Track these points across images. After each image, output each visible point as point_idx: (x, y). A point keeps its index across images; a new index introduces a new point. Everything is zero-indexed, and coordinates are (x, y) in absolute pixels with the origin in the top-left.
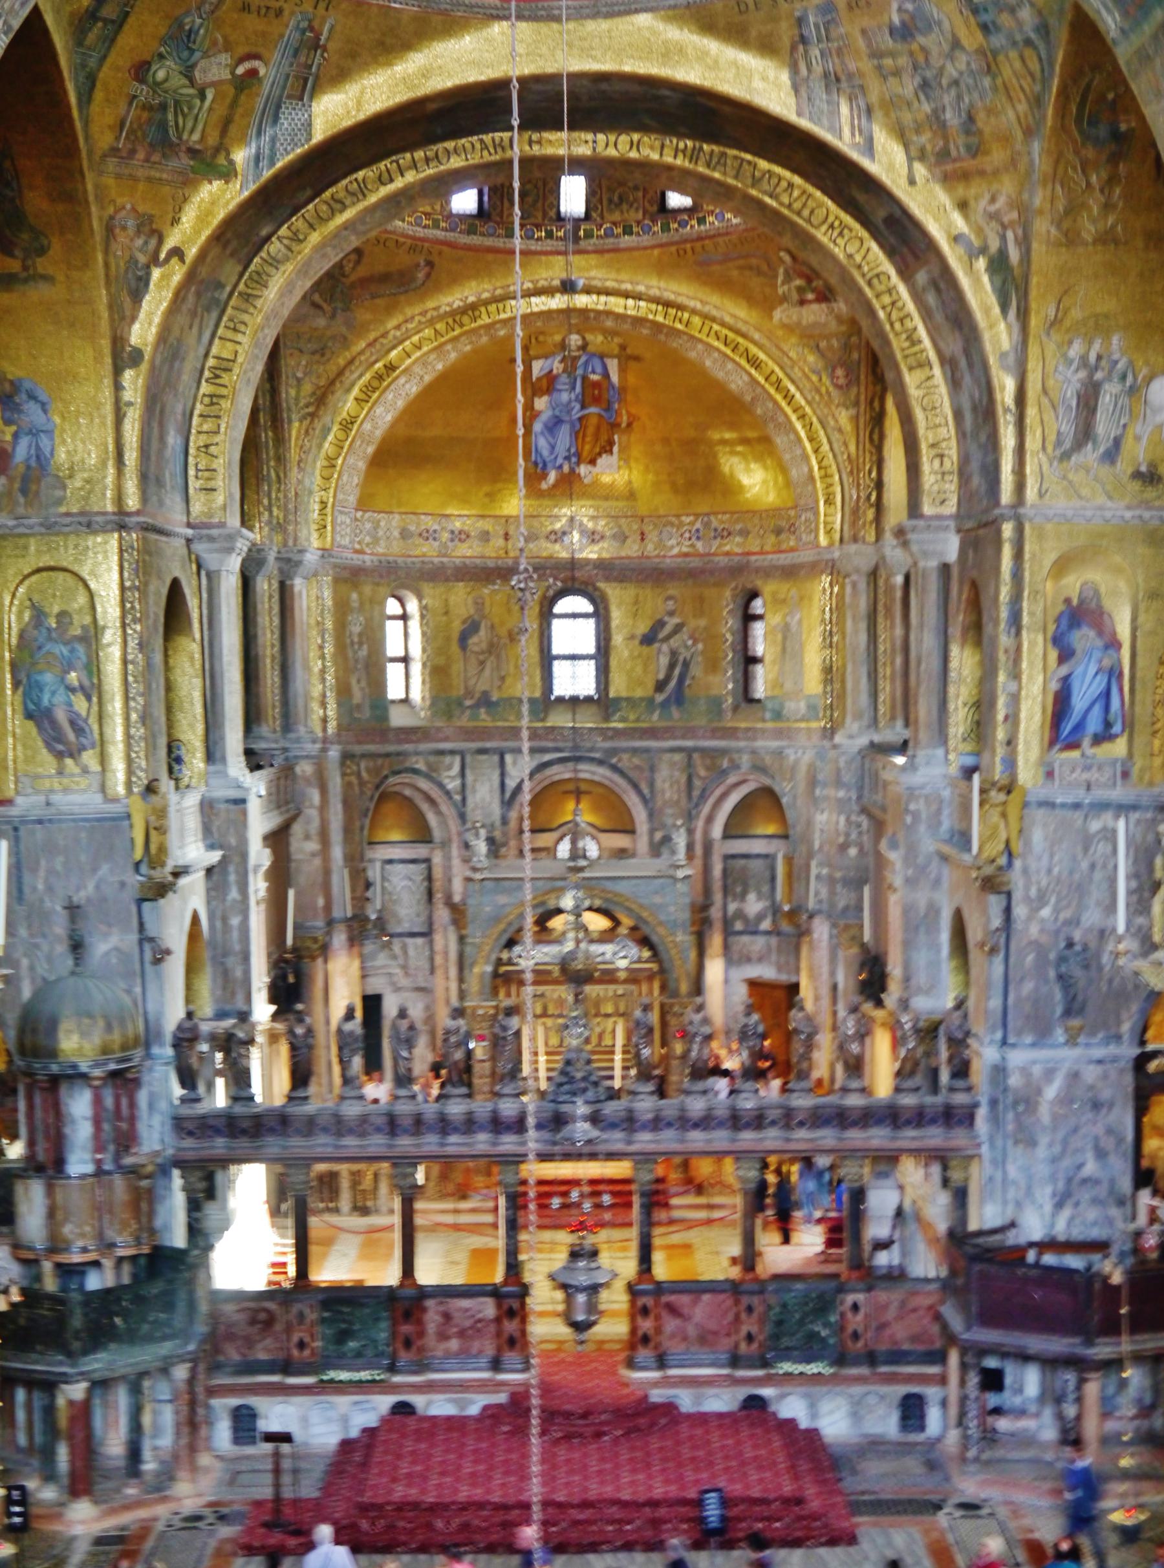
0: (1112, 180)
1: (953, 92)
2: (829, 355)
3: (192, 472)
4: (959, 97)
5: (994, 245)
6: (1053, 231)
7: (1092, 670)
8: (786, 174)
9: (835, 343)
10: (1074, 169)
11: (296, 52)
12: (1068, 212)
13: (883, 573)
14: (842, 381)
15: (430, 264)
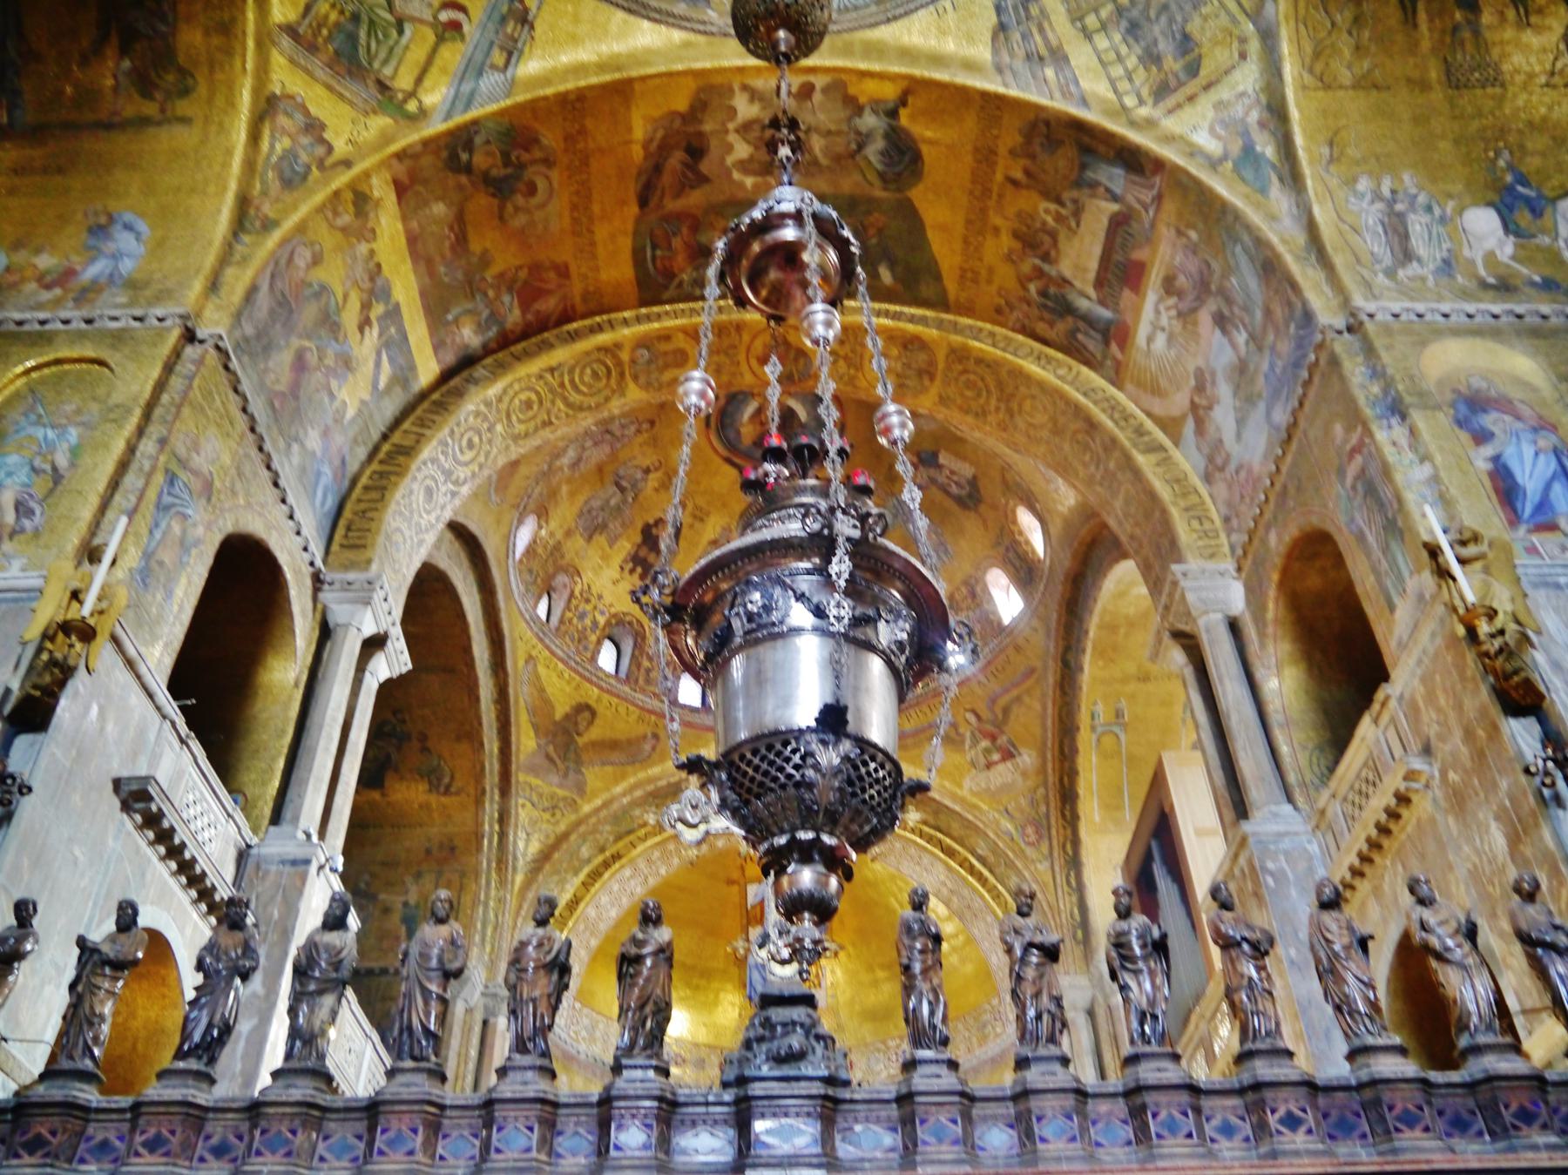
0: (1357, 20)
1: (1163, 19)
2: (1017, 814)
3: (340, 531)
4: (1171, 21)
5: (1236, 147)
6: (1306, 75)
7: (1528, 451)
8: (988, 326)
9: (1023, 802)
10: (1316, 8)
11: (503, 20)
12: (1317, 55)
13: (1100, 999)
14: (1033, 838)
15: (656, 736)
